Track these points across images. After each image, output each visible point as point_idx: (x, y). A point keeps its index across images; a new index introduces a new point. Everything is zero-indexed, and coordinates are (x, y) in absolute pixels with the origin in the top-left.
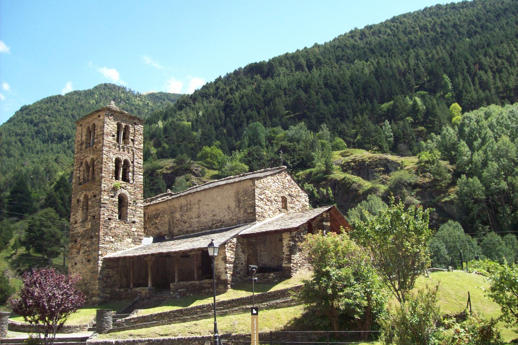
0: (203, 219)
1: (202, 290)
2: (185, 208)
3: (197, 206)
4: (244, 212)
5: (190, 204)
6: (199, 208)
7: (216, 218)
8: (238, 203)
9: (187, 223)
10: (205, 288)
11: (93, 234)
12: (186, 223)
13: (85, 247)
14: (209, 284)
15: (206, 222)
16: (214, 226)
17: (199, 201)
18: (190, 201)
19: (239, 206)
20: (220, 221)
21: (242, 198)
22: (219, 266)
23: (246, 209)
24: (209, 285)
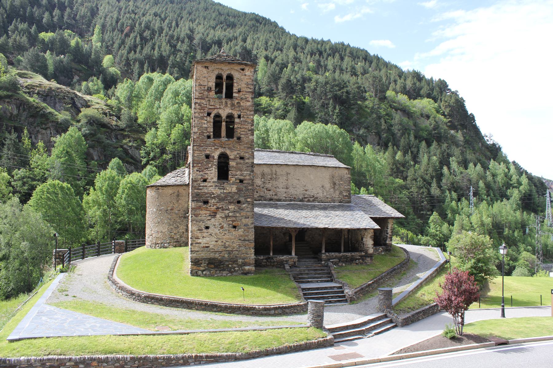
0: (292, 191)
1: (352, 261)
2: (269, 177)
3: (285, 178)
4: (340, 194)
5: (276, 174)
6: (287, 180)
7: (307, 193)
8: (333, 185)
9: (272, 191)
10: (357, 259)
11: (242, 199)
12: (270, 190)
13: (227, 212)
14: (359, 256)
15: (296, 195)
16: (306, 200)
17: (288, 174)
18: (276, 172)
19: (334, 188)
20: (314, 196)
21: (337, 182)
22: (368, 243)
23: (341, 191)
24: (360, 257)
